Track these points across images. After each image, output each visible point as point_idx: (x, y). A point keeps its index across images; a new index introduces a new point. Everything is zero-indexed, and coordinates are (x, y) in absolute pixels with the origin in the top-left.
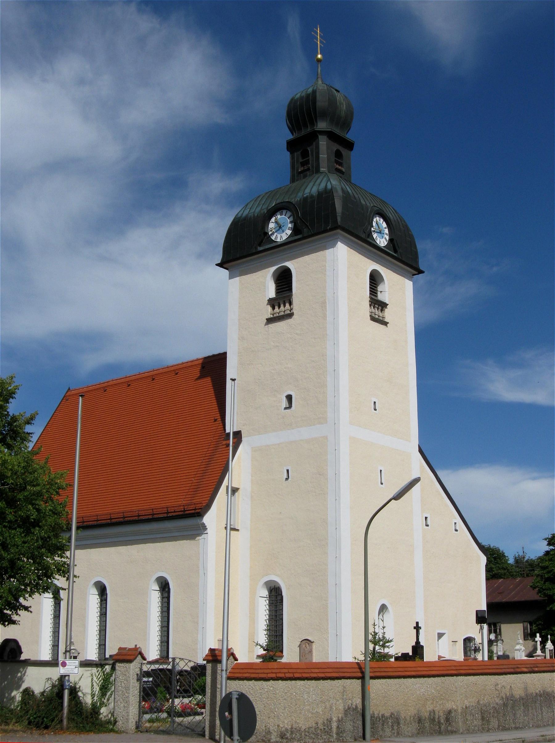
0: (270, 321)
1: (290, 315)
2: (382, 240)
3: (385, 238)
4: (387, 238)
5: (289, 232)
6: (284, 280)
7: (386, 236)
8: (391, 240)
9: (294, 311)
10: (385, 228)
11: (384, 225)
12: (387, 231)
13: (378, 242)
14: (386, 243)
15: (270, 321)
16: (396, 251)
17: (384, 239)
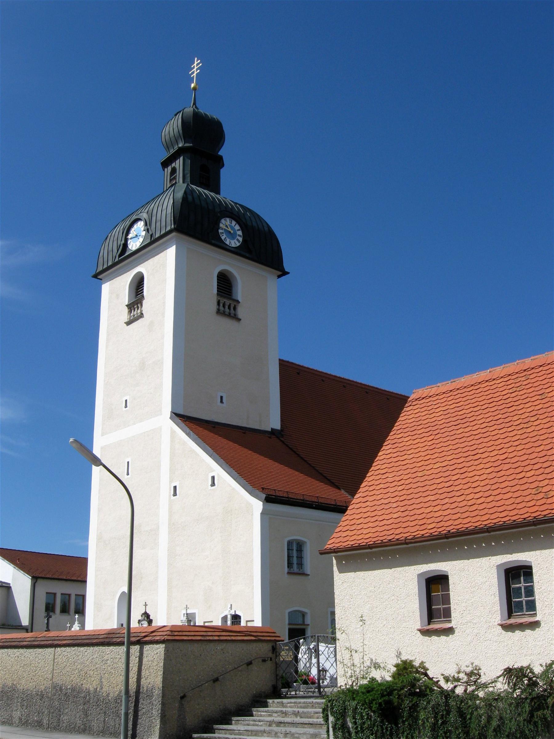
0: (128, 323)
1: (141, 316)
2: (233, 242)
3: (238, 240)
4: (241, 239)
5: (141, 240)
6: (138, 285)
7: (238, 237)
9: (143, 312)
10: (238, 230)
11: (237, 227)
12: (240, 233)
13: (227, 242)
14: (238, 244)
15: (128, 323)
17: (235, 241)
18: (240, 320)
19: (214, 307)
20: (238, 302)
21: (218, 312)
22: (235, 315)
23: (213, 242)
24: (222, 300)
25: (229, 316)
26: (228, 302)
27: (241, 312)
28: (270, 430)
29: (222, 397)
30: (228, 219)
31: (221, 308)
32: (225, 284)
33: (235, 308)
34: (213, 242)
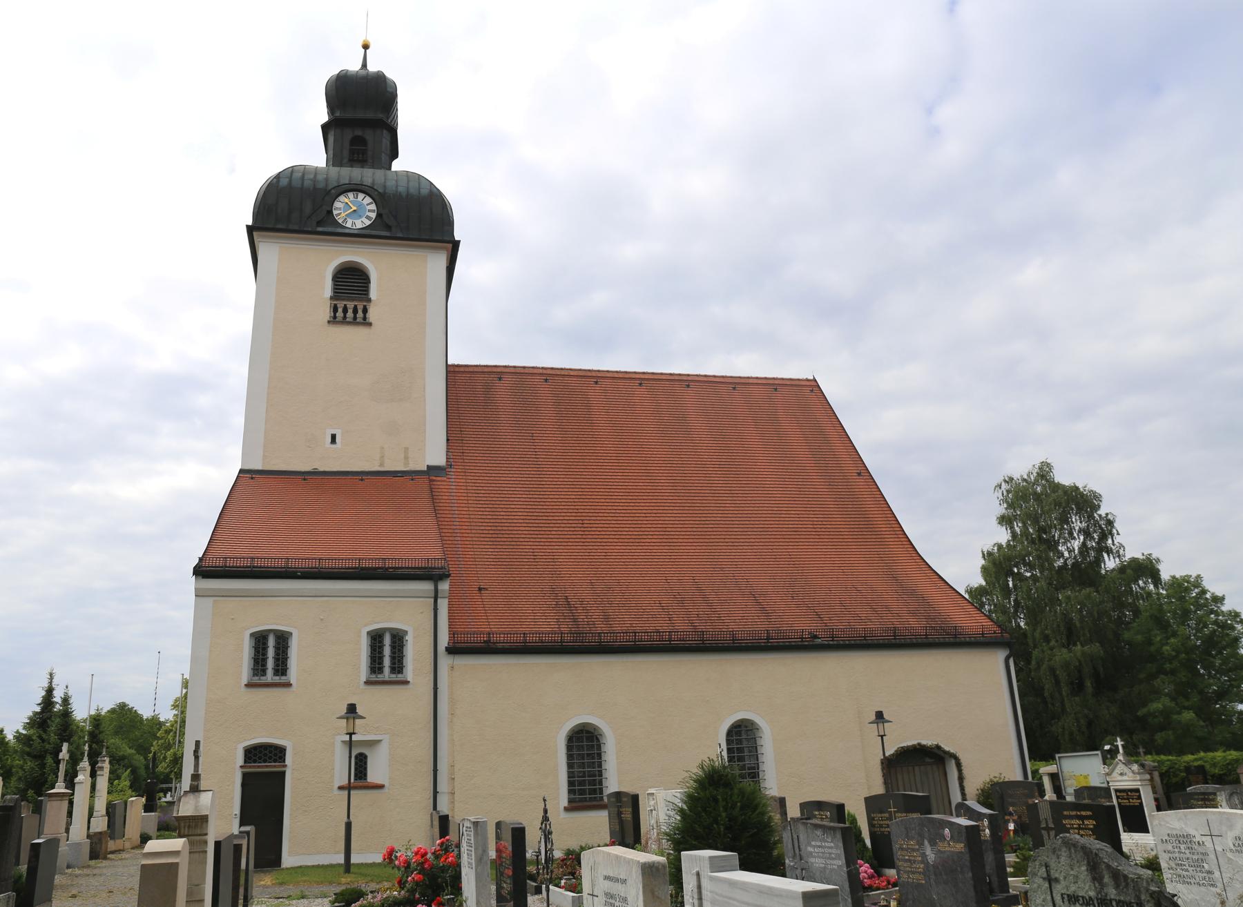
3: (368, 218)
4: (373, 215)
8: (379, 215)
11: (368, 200)
12: (373, 207)
13: (349, 225)
14: (368, 223)
16: (389, 228)
18: (370, 324)
19: (326, 313)
20: (369, 300)
21: (333, 320)
22: (365, 318)
23: (320, 229)
24: (340, 305)
25: (354, 322)
26: (350, 305)
27: (372, 315)
28: (425, 469)
29: (334, 438)
30: (351, 195)
31: (340, 314)
32: (351, 283)
33: (365, 311)
34: (320, 229)
